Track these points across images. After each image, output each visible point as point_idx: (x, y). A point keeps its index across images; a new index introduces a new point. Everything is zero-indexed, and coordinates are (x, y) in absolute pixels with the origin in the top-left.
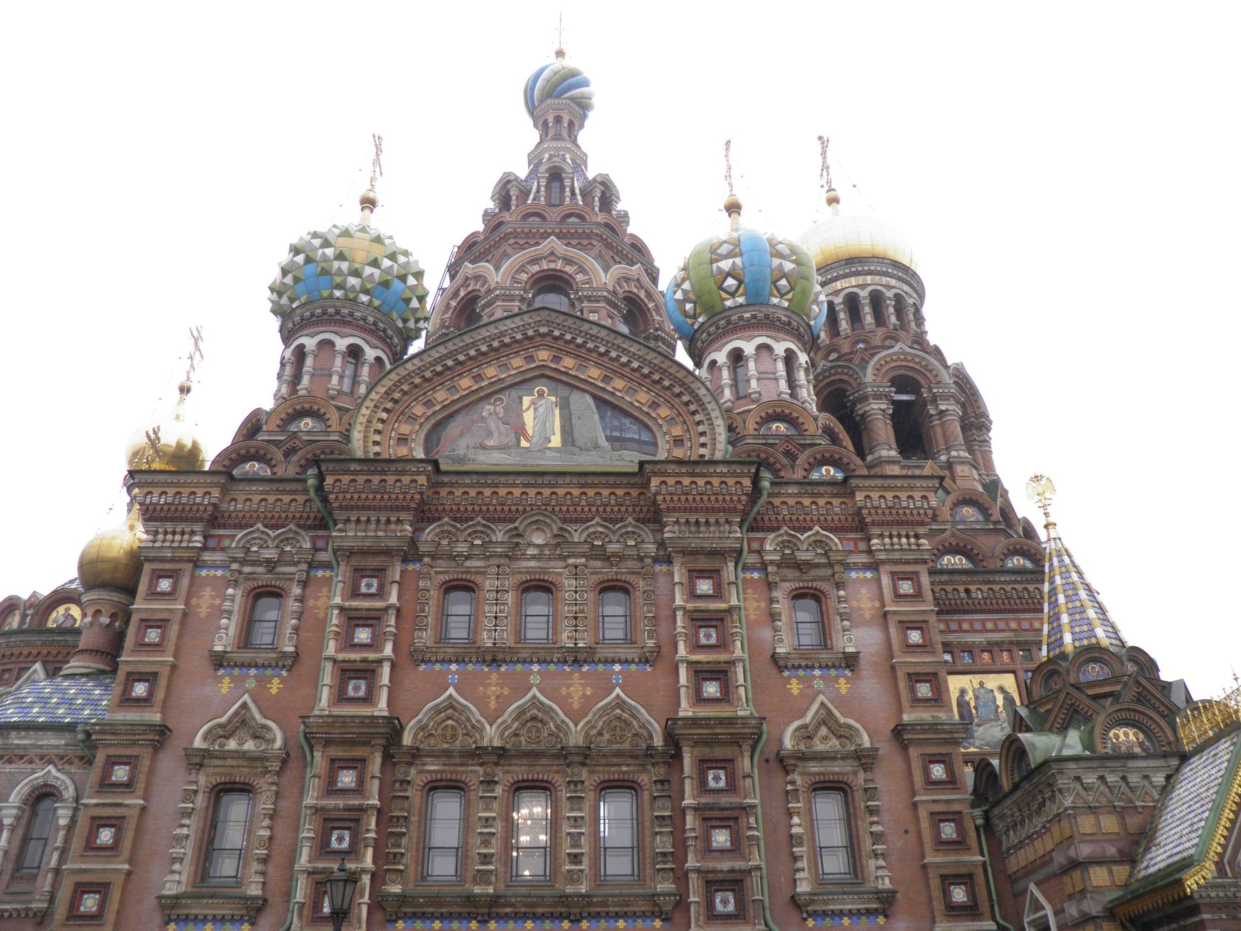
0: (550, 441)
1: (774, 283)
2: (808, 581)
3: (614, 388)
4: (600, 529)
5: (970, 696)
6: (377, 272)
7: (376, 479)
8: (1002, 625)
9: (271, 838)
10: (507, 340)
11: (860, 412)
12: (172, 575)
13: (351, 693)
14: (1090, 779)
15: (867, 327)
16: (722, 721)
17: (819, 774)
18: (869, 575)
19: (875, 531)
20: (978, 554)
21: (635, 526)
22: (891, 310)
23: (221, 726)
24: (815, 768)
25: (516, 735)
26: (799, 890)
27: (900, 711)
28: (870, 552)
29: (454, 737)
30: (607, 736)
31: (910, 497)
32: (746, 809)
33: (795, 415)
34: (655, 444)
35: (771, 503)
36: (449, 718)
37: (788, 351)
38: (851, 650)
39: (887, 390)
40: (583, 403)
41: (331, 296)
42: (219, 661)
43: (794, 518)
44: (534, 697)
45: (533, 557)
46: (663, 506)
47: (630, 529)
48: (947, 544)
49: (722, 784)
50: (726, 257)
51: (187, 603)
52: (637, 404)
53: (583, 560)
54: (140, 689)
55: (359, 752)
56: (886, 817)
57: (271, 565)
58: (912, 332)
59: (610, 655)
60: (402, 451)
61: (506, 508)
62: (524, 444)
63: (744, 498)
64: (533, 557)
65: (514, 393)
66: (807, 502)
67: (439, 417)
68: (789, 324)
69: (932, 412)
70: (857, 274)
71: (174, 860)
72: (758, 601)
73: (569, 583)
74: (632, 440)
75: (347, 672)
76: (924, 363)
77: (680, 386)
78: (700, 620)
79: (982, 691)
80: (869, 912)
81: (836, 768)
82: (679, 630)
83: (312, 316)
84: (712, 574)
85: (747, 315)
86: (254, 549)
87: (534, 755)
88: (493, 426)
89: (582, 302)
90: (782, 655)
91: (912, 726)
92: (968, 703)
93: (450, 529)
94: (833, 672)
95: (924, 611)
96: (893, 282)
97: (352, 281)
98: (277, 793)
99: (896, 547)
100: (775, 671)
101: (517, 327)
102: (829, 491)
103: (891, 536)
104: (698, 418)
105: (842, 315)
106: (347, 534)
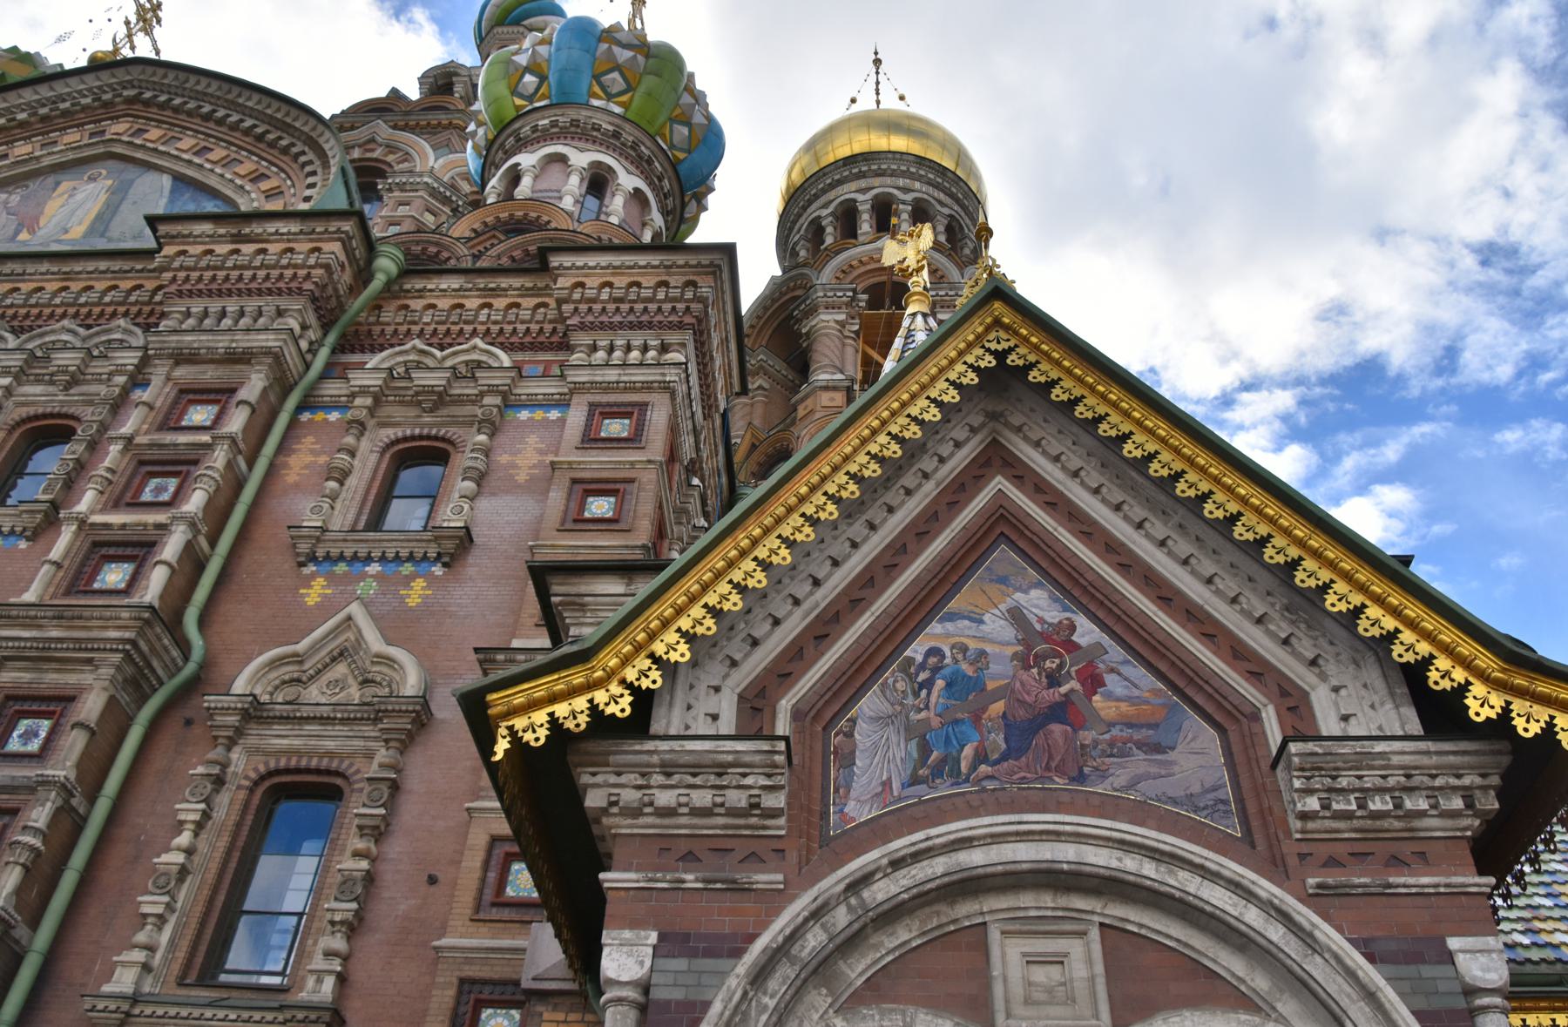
0: (66, 232)
2: (431, 426)
3: (208, 160)
11: (804, 331)
17: (289, 752)
18: (554, 414)
19: (583, 339)
21: (125, 331)
24: (281, 739)
26: (107, 988)
33: (545, 218)
35: (406, 307)
37: (599, 163)
39: (850, 294)
43: (442, 328)
56: (396, 847)
63: (320, 271)
65: (51, 180)
66: (472, 303)
68: (616, 135)
77: (305, 143)
81: (331, 742)
84: (221, 395)
90: (305, 532)
94: (408, 568)
95: (632, 463)
96: (917, 185)
100: (288, 565)
102: (519, 285)
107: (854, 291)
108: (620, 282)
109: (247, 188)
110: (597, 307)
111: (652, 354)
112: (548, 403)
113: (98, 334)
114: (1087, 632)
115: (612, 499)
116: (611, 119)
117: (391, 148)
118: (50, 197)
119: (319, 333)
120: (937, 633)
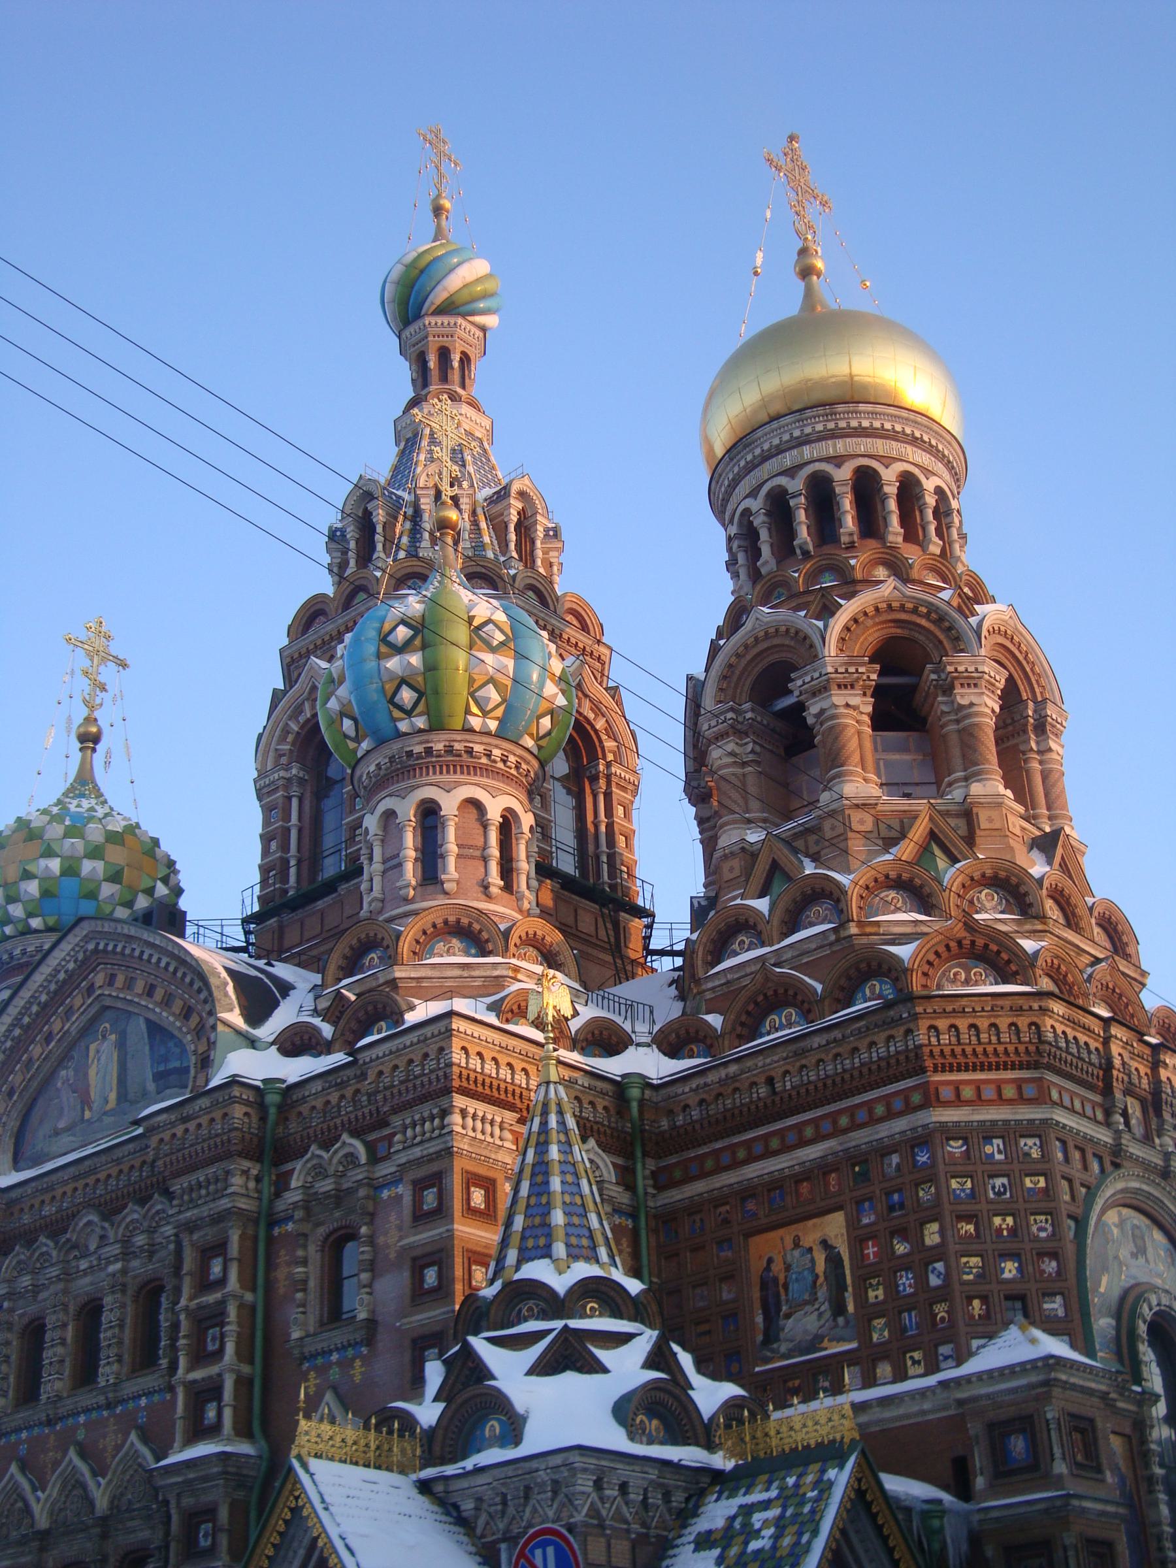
1: (391, 701)
4: (136, 1216)
5: (777, 1268)
8: (826, 1127)
10: (62, 976)
15: (764, 571)
18: (400, 1189)
19: (396, 1121)
20: (803, 1002)
21: (162, 1203)
22: (801, 515)
25: (61, 1510)
30: (130, 1496)
35: (300, 1113)
36: (16, 1501)
37: (424, 802)
39: (730, 715)
43: (325, 1126)
44: (71, 1461)
45: (85, 1273)
47: (159, 1207)
48: (760, 998)
52: (171, 1019)
53: (118, 1266)
58: (844, 539)
59: (135, 1389)
61: (64, 1214)
62: (87, 1115)
63: (233, 1134)
64: (85, 1273)
67: (20, 1106)
68: (429, 751)
69: (810, 721)
70: (751, 467)
72: (289, 1264)
73: (108, 1300)
74: (177, 1071)
76: (792, 631)
79: (797, 1253)
82: (182, 1342)
84: (219, 1248)
85: (372, 768)
88: (65, 1099)
92: (776, 1279)
93: (22, 1257)
94: (350, 1352)
96: (807, 452)
99: (418, 1139)
101: (68, 954)
107: (732, 709)
109: (184, 1029)
110: (395, 1091)
111: (437, 1121)
112: (396, 1182)
113: (149, 1210)
115: (436, 1268)
116: (417, 739)
118: (87, 1067)
119: (258, 1166)
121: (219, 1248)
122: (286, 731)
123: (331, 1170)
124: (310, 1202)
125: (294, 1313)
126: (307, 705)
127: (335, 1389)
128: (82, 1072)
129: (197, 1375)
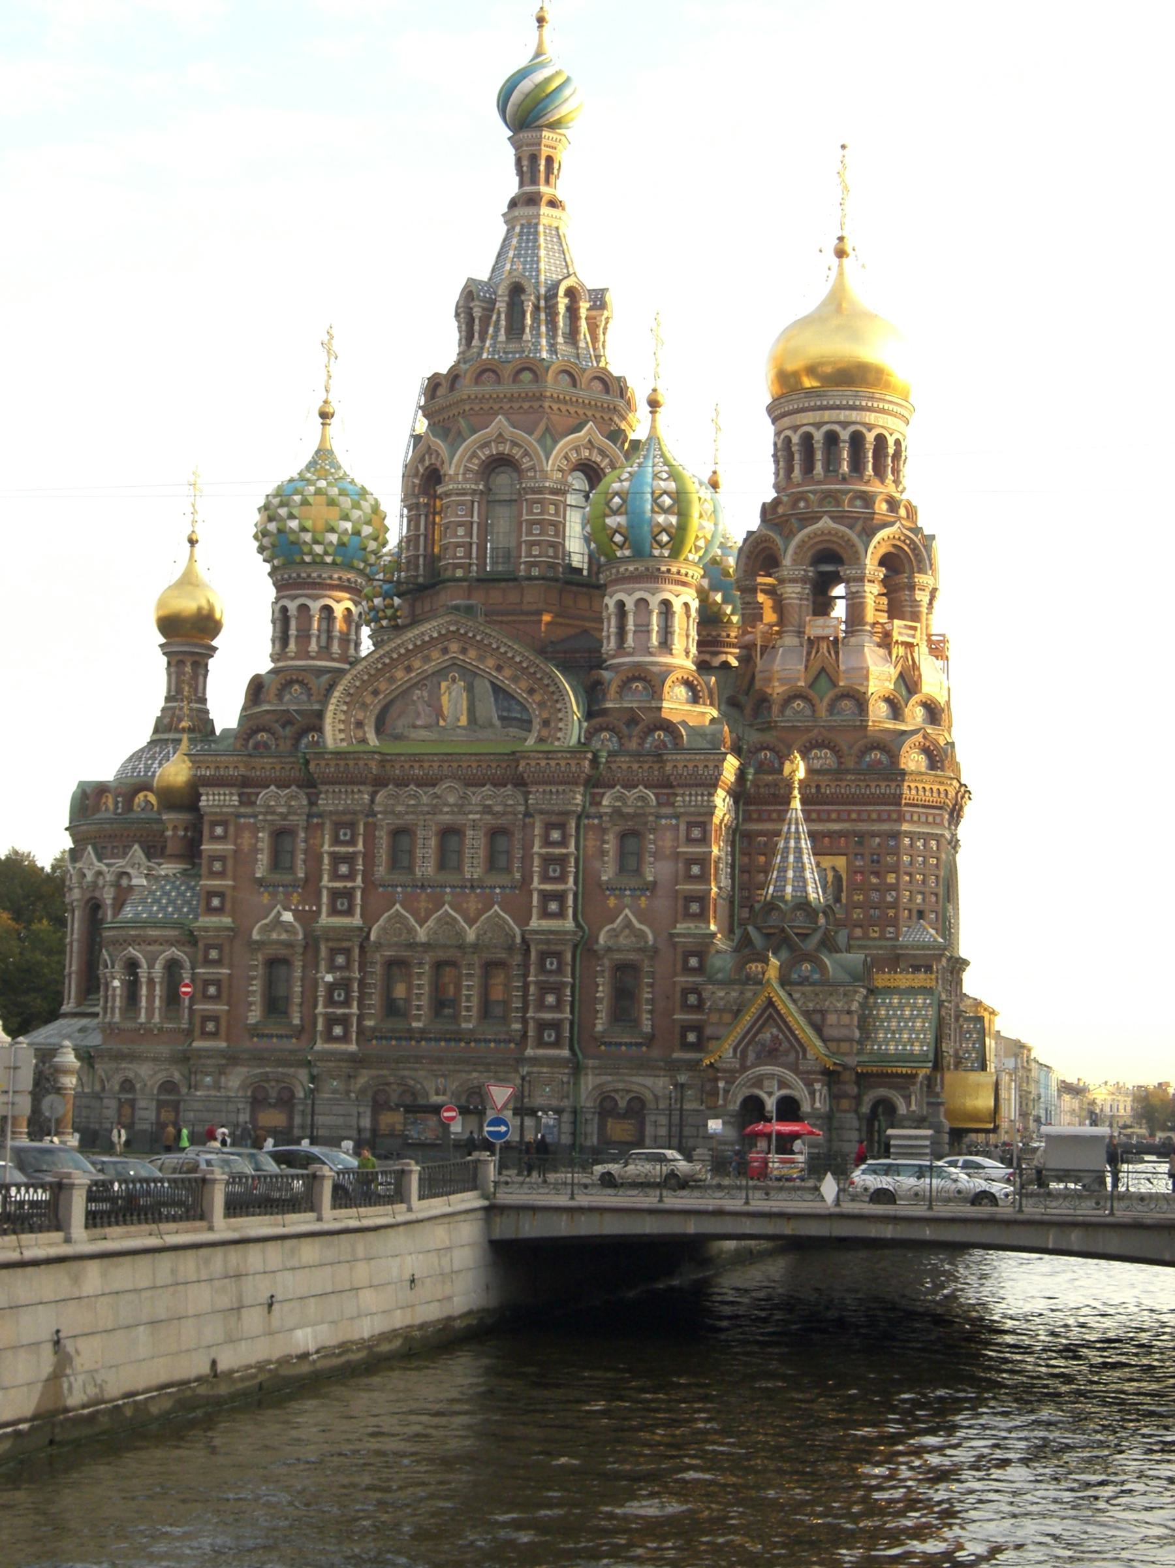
6: (333, 538)
7: (342, 763)
8: (844, 816)
9: (302, 993)
10: (427, 638)
12: (224, 824)
13: (339, 907)
14: (722, 994)
16: (551, 932)
18: (674, 822)
19: (680, 791)
23: (266, 925)
25: (435, 933)
27: (676, 922)
28: (672, 805)
29: (400, 935)
31: (706, 766)
32: (564, 984)
34: (530, 722)
38: (650, 878)
40: (483, 687)
41: (303, 562)
42: (260, 882)
45: (447, 813)
46: (528, 781)
49: (554, 967)
50: (615, 513)
51: (235, 844)
53: (478, 816)
54: (216, 902)
55: (345, 944)
57: (284, 817)
60: (360, 734)
62: (442, 723)
64: (447, 813)
65: (435, 680)
66: (635, 766)
67: (383, 703)
71: (251, 1004)
74: (515, 719)
75: (335, 894)
78: (547, 860)
80: (636, 1044)
81: (632, 956)
83: (290, 577)
85: (631, 568)
86: (273, 803)
87: (445, 947)
89: (527, 493)
91: (679, 935)
94: (638, 893)
97: (318, 549)
98: (304, 967)
103: (690, 795)
104: (559, 706)
105: (797, 457)
106: (325, 803)
108: (691, 766)
114: (781, 1036)
117: (514, 444)
120: (760, 1036)
121: (562, 826)
122: (474, 455)
123: (629, 803)
124: (617, 813)
125: (597, 864)
126: (493, 444)
127: (630, 908)
128: (435, 696)
129: (548, 887)
